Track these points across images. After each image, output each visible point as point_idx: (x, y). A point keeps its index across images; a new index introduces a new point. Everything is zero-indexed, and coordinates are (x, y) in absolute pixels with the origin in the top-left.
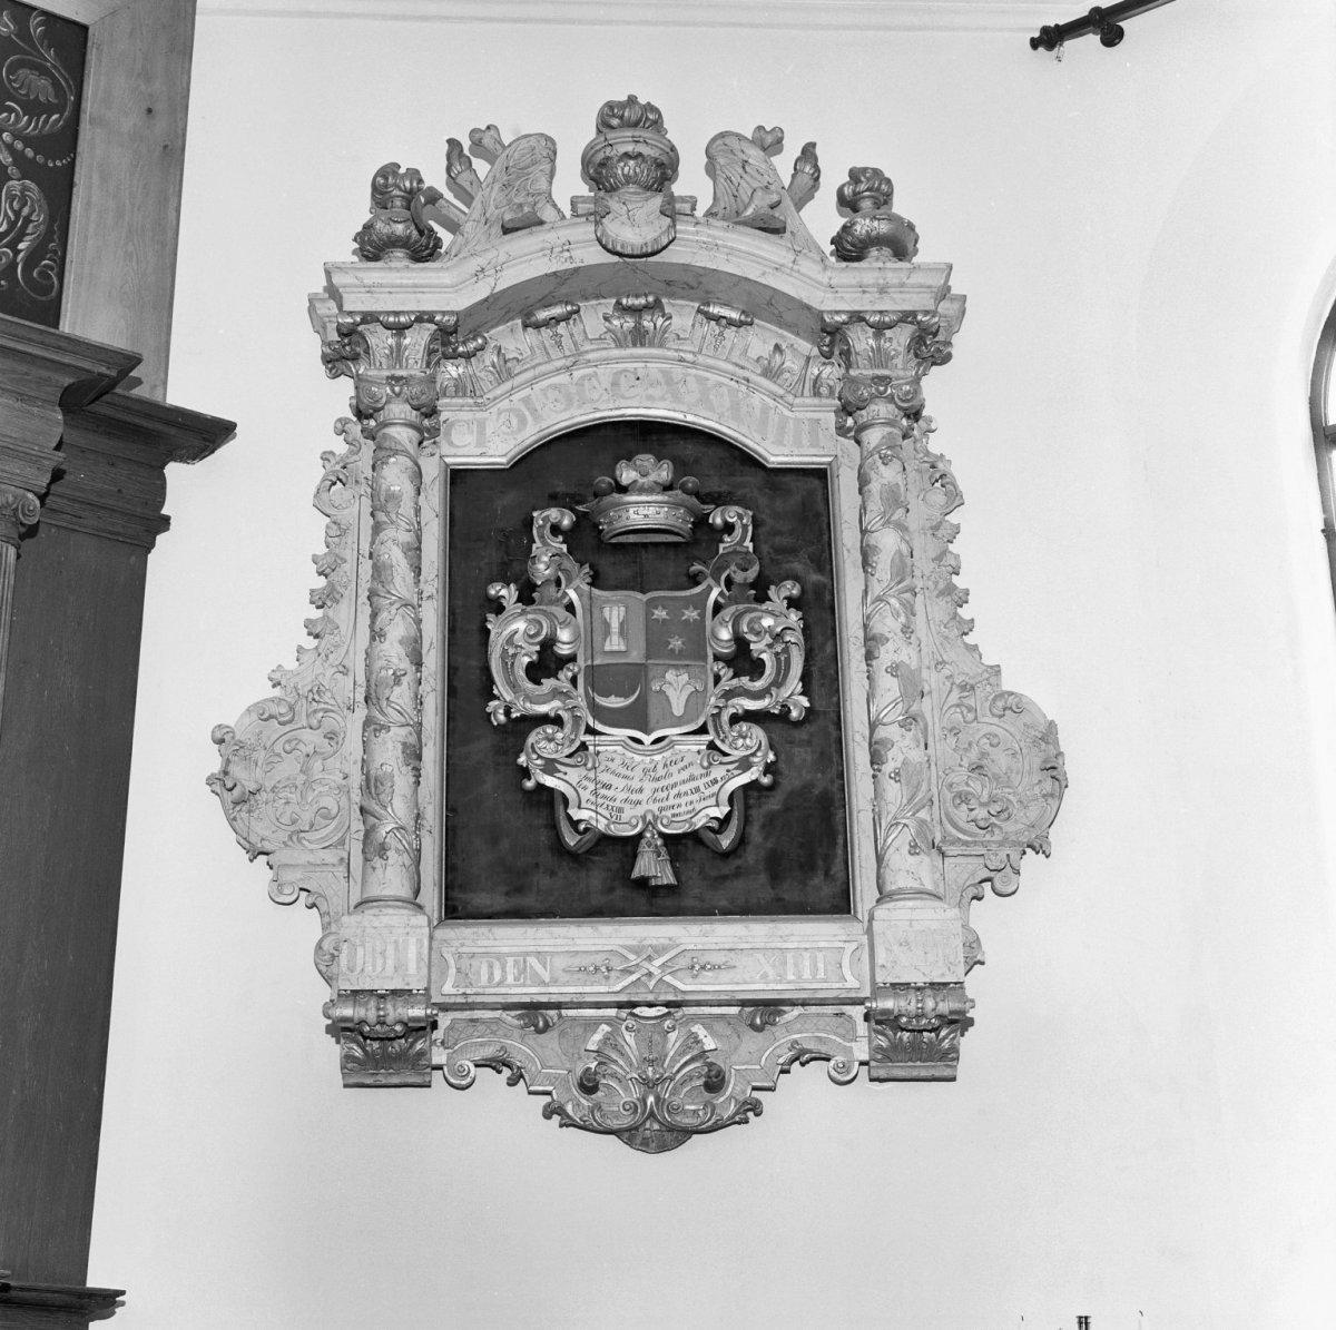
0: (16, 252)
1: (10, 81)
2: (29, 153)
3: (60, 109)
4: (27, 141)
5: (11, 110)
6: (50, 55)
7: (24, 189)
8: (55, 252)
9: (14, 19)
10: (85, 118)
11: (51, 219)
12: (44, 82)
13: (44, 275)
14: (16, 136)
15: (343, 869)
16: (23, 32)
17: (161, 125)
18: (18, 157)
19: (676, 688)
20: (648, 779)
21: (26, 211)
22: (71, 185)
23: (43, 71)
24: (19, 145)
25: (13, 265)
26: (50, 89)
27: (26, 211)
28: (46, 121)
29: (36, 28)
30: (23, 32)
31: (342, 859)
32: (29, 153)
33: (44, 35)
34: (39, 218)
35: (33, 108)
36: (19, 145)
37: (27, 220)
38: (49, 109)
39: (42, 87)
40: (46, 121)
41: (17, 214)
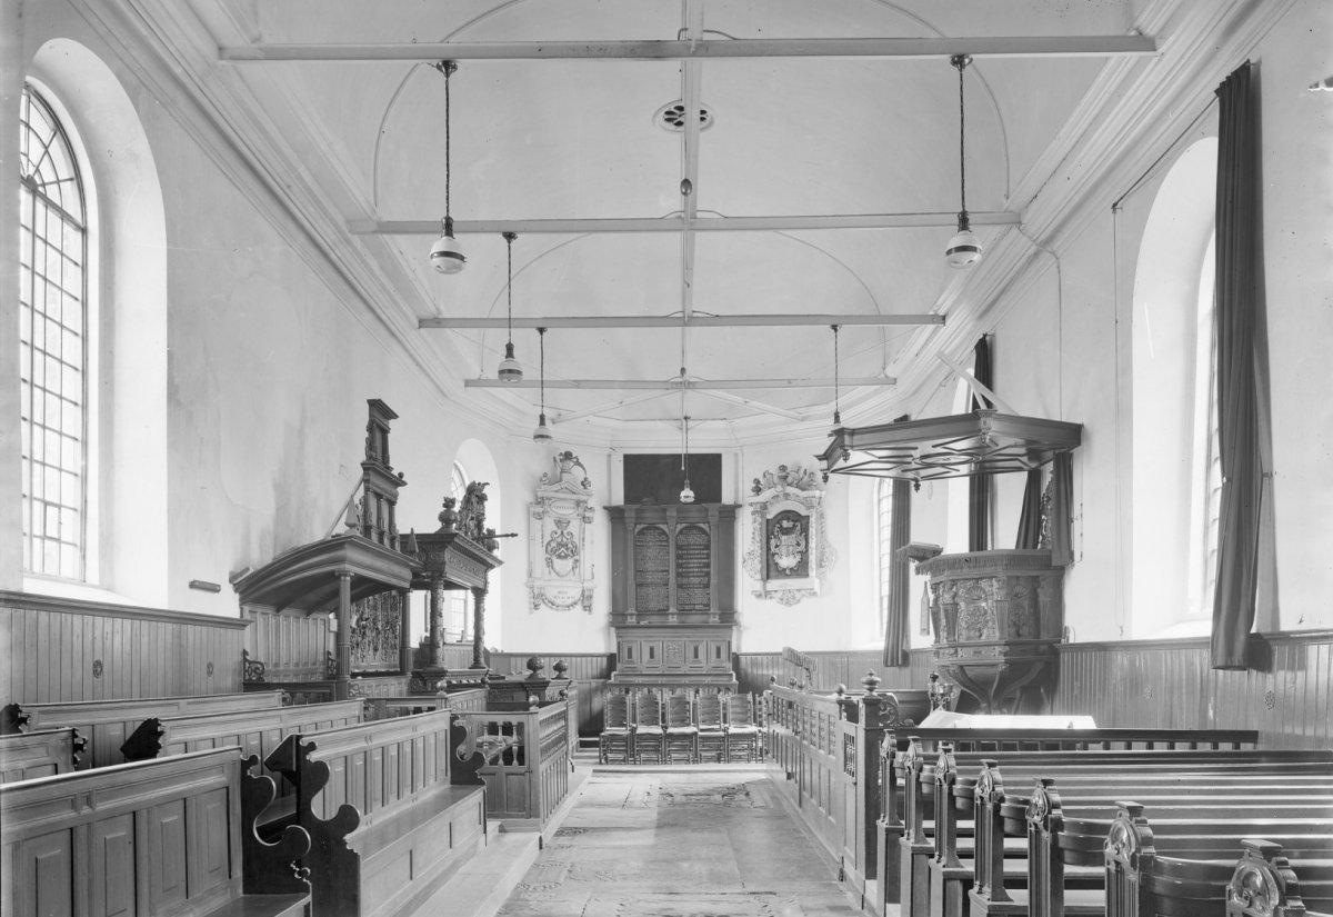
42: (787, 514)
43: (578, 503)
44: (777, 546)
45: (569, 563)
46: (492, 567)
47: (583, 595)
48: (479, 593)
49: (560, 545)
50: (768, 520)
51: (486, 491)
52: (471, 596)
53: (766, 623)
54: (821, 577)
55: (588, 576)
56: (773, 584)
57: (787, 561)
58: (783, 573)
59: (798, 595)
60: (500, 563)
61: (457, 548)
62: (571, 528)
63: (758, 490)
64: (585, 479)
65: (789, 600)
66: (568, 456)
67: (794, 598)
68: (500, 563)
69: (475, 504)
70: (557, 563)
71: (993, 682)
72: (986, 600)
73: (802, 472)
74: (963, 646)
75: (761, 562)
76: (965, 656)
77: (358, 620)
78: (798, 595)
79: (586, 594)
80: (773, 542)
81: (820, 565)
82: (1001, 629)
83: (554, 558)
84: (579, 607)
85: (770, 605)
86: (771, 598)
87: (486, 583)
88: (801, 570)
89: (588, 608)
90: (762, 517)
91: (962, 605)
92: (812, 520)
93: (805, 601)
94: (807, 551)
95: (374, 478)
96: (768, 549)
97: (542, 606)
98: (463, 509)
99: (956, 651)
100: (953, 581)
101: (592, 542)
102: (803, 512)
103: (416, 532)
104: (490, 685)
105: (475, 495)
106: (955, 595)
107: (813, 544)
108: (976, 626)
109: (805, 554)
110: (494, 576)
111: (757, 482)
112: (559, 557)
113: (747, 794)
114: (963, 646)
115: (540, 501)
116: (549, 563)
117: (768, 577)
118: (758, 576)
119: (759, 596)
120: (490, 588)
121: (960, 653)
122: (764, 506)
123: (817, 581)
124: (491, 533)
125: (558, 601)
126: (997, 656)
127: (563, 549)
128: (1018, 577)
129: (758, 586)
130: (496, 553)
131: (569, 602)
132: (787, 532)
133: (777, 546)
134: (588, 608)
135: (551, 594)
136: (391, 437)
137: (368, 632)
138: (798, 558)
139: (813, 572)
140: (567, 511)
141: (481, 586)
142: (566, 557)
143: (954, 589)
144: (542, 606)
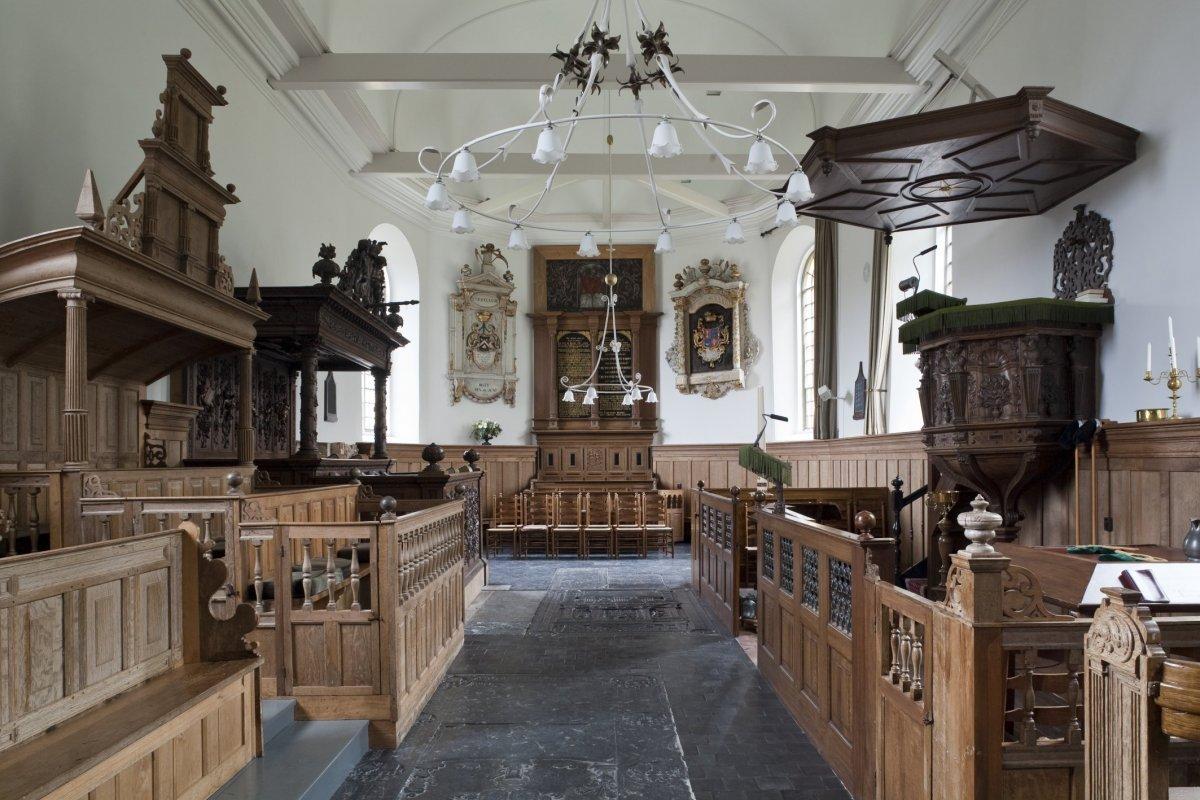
19: (714, 342)
20: (711, 355)
42: (713, 308)
43: (499, 296)
44: (700, 340)
45: (492, 354)
46: (396, 346)
47: (504, 389)
48: (381, 373)
49: (482, 337)
50: (691, 315)
51: (384, 253)
52: (368, 380)
53: (692, 420)
54: (745, 366)
55: (510, 370)
56: (696, 378)
57: (711, 355)
58: (707, 367)
59: (723, 388)
60: (405, 342)
61: (340, 312)
62: (493, 322)
63: (680, 285)
64: (508, 272)
65: (715, 392)
66: (490, 248)
67: (718, 391)
68: (405, 342)
69: (370, 270)
70: (480, 357)
71: (1015, 474)
72: (1008, 368)
73: (724, 264)
74: (975, 429)
75: (685, 356)
76: (978, 443)
77: (217, 397)
78: (723, 388)
79: (508, 387)
80: (696, 336)
81: (744, 356)
82: (1031, 409)
83: (476, 353)
84: (500, 401)
85: (696, 399)
86: (696, 392)
87: (388, 363)
88: (726, 362)
89: (511, 401)
90: (685, 312)
91: (976, 375)
92: (737, 311)
93: (732, 394)
94: (731, 343)
95: (171, 176)
96: (692, 343)
97: (463, 399)
98: (349, 264)
99: (966, 437)
100: (962, 342)
101: (514, 335)
102: (726, 305)
103: (262, 283)
104: (364, 480)
105: (369, 256)
106: (965, 361)
107: (737, 336)
108: (993, 405)
109: (729, 347)
110: (397, 355)
111: (679, 277)
112: (481, 349)
113: (679, 607)
114: (975, 429)
115: (460, 294)
116: (470, 355)
117: (692, 372)
118: (682, 371)
119: (683, 390)
120: (394, 369)
121: (971, 438)
122: (687, 301)
123: (742, 373)
124: (395, 307)
125: (480, 394)
126: (1024, 442)
127: (483, 340)
128: (1047, 338)
129: (682, 380)
130: (400, 330)
131: (491, 394)
132: (707, 325)
133: (700, 340)
134: (511, 401)
135: (472, 387)
136: (212, 129)
137: (233, 411)
138: (722, 349)
139: (737, 364)
140: (488, 303)
141: (382, 365)
142: (487, 349)
143: (964, 353)
144: (463, 399)
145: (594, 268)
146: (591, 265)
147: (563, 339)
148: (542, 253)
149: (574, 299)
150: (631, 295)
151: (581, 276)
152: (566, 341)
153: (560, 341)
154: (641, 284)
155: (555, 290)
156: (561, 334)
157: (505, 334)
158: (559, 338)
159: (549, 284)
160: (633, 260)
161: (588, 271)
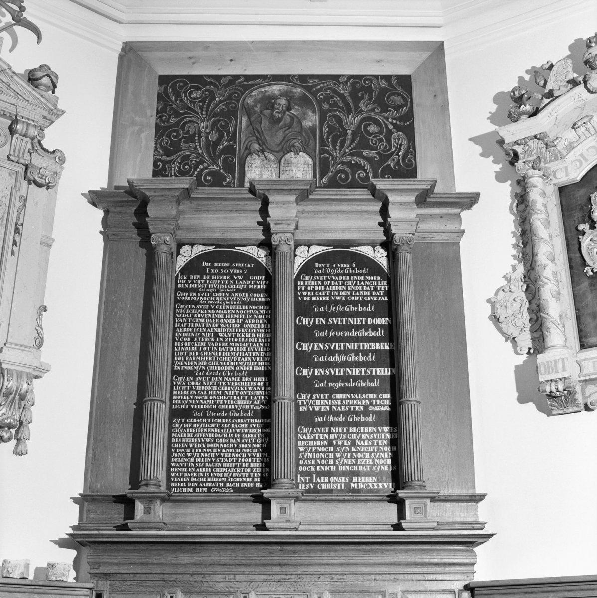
0: (399, 156)
1: (388, 101)
2: (398, 123)
3: (406, 105)
4: (396, 119)
5: (390, 111)
6: (400, 89)
7: (399, 135)
8: (412, 152)
9: (386, 81)
10: (415, 105)
11: (409, 141)
12: (399, 98)
13: (410, 161)
14: (393, 119)
15: (541, 338)
16: (390, 84)
17: (440, 99)
18: (394, 125)
21: (400, 142)
22: (414, 128)
23: (399, 94)
24: (394, 121)
25: (399, 160)
26: (402, 100)
27: (400, 142)
28: (402, 111)
29: (394, 81)
30: (390, 84)
31: (540, 335)
32: (398, 123)
33: (397, 83)
34: (405, 143)
35: (397, 108)
36: (394, 121)
37: (401, 145)
38: (402, 106)
39: (399, 100)
40: (402, 111)
41: (397, 144)
101: (47, 243)
145: (284, 94)
146: (275, 89)
147: (193, 267)
148: (145, 55)
149: (229, 168)
150: (384, 157)
151: (249, 112)
152: (202, 272)
153: (182, 271)
154: (410, 132)
155: (176, 144)
156: (187, 254)
157: (17, 231)
158: (181, 262)
159: (160, 131)
160: (387, 78)
161: (269, 102)
